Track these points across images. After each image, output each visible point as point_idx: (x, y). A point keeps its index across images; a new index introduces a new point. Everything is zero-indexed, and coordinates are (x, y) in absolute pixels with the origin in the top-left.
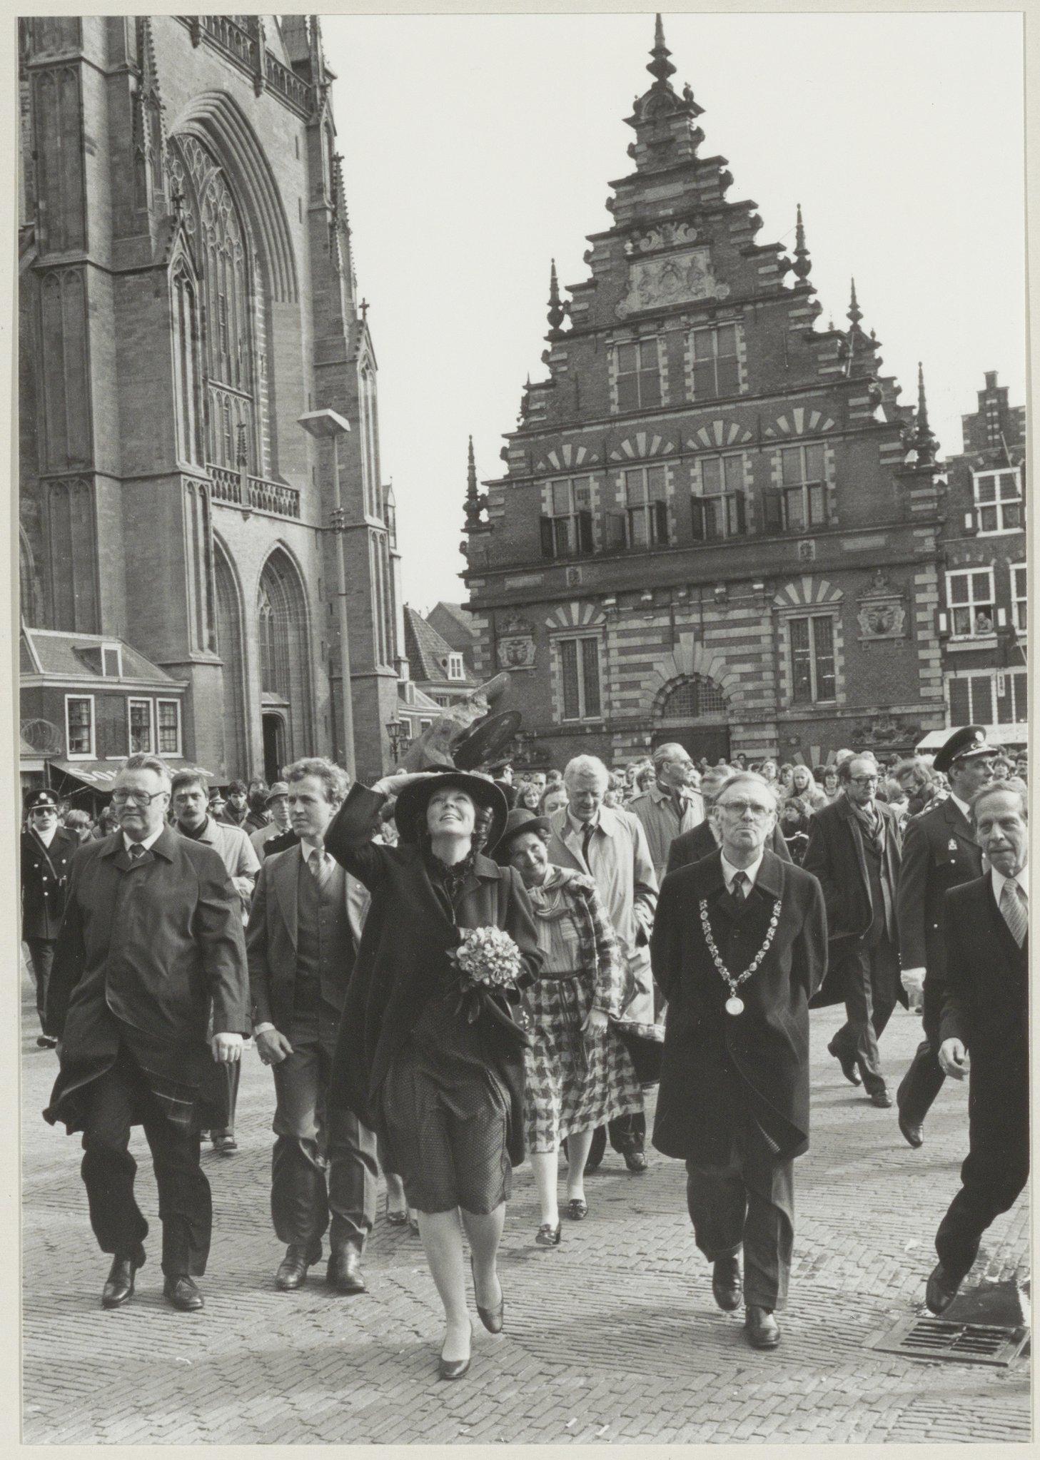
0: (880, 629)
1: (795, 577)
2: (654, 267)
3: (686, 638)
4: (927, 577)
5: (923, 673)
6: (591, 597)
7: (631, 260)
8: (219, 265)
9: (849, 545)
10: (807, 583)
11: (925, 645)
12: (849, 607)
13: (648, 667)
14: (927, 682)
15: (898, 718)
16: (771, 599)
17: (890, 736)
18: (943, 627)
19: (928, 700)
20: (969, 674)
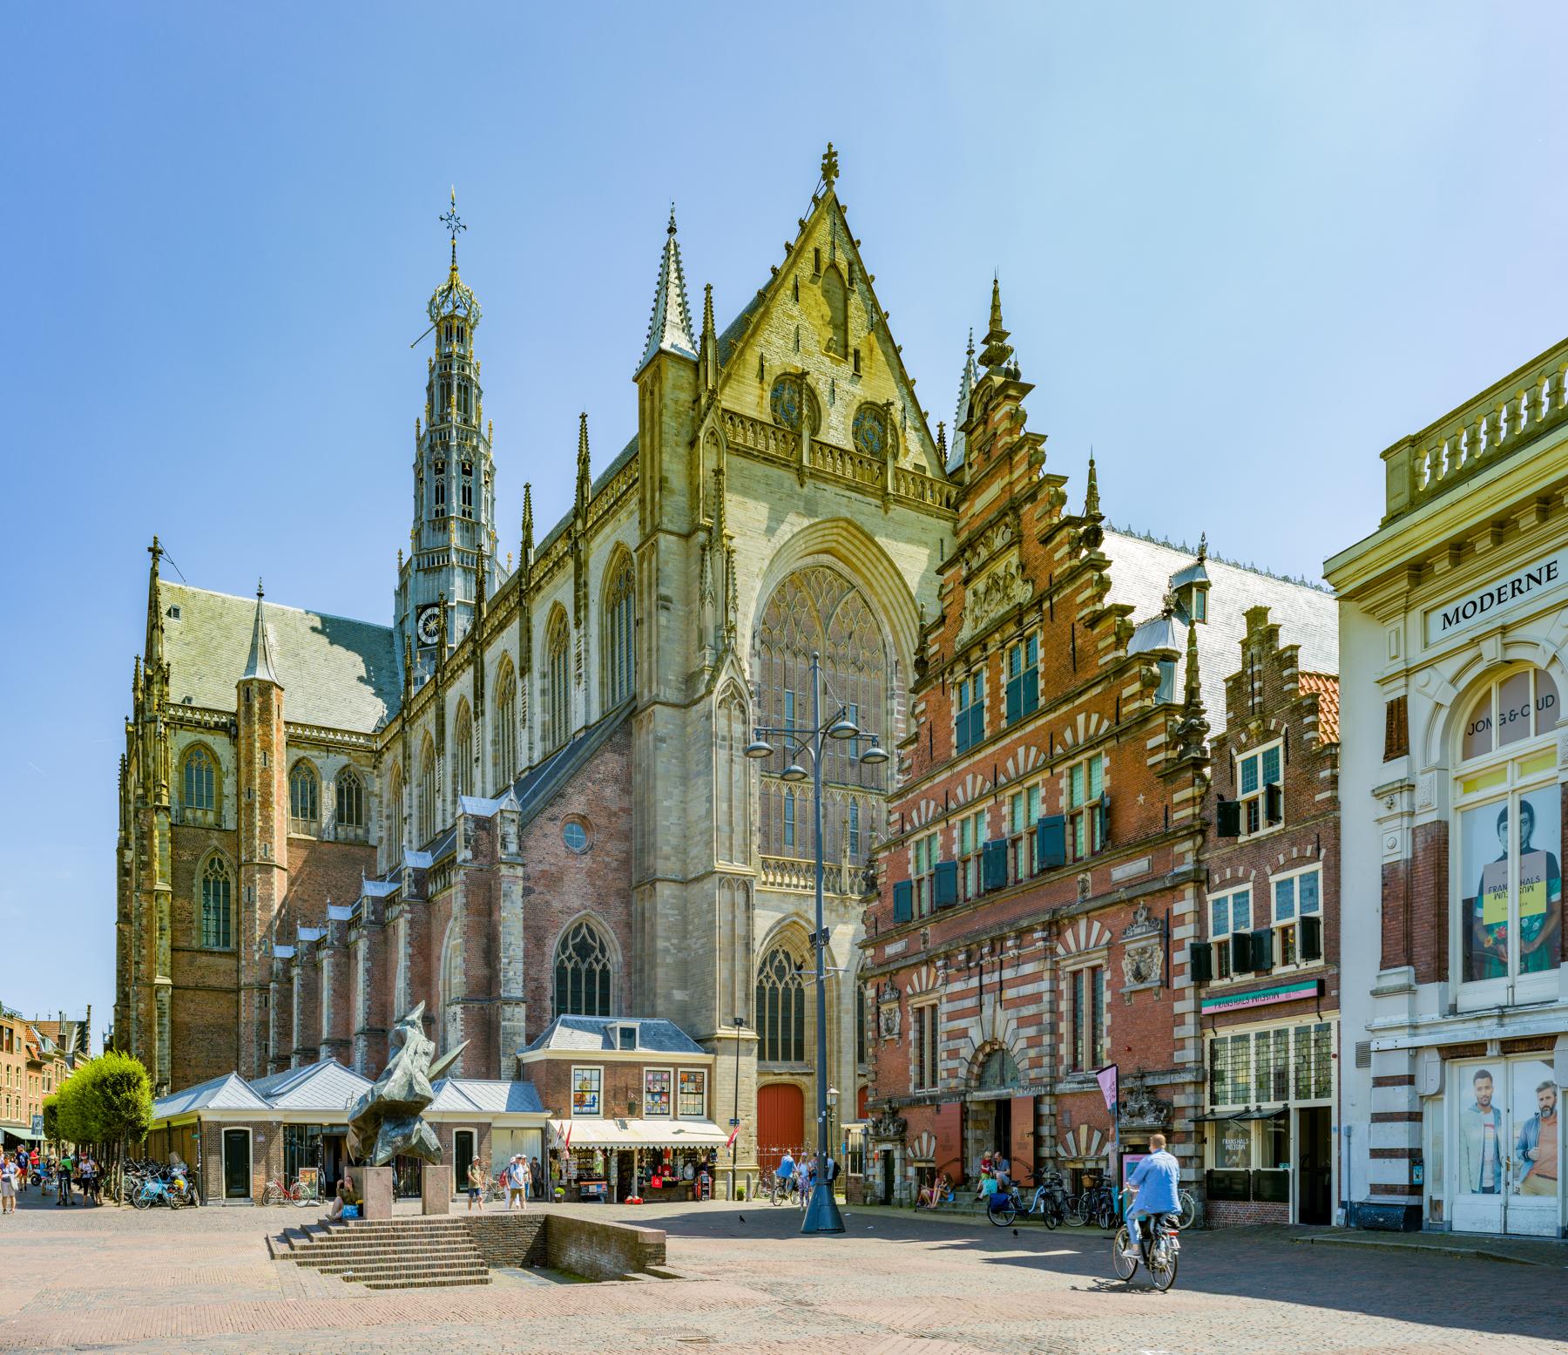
0: (1139, 976)
1: (1073, 920)
5: (1179, 1033)
10: (1083, 924)
11: (1180, 995)
12: (1114, 949)
14: (1180, 1044)
20: (1226, 1032)
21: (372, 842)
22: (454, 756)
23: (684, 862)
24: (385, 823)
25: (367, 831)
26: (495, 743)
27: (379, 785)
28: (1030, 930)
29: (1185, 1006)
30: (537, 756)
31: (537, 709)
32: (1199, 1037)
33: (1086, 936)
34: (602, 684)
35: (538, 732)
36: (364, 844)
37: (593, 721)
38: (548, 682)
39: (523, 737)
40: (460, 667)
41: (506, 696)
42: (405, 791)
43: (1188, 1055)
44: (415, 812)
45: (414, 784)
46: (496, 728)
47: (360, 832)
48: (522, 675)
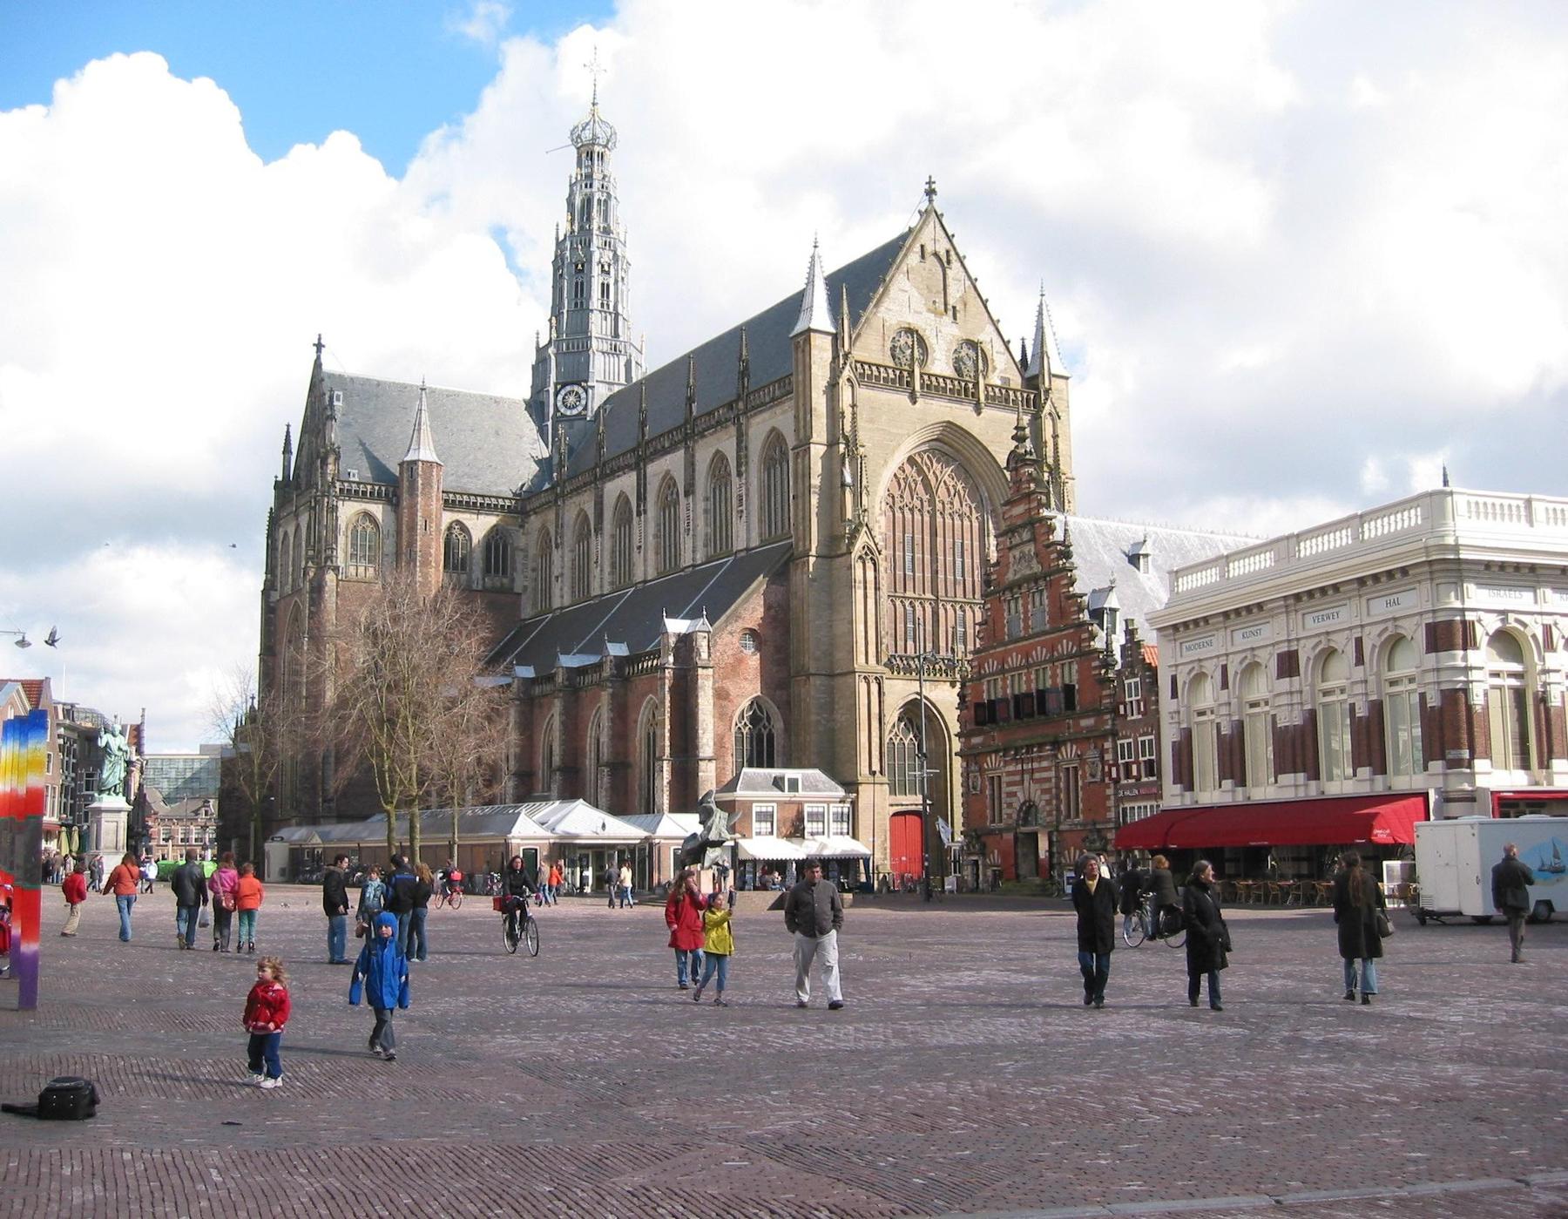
0: (1093, 776)
1: (1064, 743)
2: (1017, 553)
3: (1026, 777)
4: (1108, 745)
6: (996, 752)
7: (1010, 549)
8: (958, 522)
9: (1084, 723)
13: (1014, 794)
15: (1099, 831)
16: (1055, 756)
17: (1093, 841)
18: (1114, 775)
19: (1109, 821)
20: (1128, 805)
21: (518, 589)
22: (613, 536)
23: (832, 663)
24: (530, 574)
25: (513, 580)
26: (656, 536)
27: (526, 540)
28: (1045, 744)
29: (1110, 791)
30: (700, 558)
31: (701, 522)
32: (1117, 807)
33: (1069, 752)
34: (760, 521)
35: (700, 543)
36: (509, 591)
37: (753, 545)
38: (710, 505)
39: (687, 544)
40: (619, 469)
41: (669, 503)
42: (556, 555)
43: (1112, 815)
44: (567, 572)
45: (566, 550)
46: (658, 525)
47: (505, 581)
48: (687, 494)
